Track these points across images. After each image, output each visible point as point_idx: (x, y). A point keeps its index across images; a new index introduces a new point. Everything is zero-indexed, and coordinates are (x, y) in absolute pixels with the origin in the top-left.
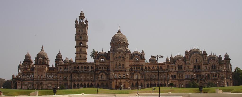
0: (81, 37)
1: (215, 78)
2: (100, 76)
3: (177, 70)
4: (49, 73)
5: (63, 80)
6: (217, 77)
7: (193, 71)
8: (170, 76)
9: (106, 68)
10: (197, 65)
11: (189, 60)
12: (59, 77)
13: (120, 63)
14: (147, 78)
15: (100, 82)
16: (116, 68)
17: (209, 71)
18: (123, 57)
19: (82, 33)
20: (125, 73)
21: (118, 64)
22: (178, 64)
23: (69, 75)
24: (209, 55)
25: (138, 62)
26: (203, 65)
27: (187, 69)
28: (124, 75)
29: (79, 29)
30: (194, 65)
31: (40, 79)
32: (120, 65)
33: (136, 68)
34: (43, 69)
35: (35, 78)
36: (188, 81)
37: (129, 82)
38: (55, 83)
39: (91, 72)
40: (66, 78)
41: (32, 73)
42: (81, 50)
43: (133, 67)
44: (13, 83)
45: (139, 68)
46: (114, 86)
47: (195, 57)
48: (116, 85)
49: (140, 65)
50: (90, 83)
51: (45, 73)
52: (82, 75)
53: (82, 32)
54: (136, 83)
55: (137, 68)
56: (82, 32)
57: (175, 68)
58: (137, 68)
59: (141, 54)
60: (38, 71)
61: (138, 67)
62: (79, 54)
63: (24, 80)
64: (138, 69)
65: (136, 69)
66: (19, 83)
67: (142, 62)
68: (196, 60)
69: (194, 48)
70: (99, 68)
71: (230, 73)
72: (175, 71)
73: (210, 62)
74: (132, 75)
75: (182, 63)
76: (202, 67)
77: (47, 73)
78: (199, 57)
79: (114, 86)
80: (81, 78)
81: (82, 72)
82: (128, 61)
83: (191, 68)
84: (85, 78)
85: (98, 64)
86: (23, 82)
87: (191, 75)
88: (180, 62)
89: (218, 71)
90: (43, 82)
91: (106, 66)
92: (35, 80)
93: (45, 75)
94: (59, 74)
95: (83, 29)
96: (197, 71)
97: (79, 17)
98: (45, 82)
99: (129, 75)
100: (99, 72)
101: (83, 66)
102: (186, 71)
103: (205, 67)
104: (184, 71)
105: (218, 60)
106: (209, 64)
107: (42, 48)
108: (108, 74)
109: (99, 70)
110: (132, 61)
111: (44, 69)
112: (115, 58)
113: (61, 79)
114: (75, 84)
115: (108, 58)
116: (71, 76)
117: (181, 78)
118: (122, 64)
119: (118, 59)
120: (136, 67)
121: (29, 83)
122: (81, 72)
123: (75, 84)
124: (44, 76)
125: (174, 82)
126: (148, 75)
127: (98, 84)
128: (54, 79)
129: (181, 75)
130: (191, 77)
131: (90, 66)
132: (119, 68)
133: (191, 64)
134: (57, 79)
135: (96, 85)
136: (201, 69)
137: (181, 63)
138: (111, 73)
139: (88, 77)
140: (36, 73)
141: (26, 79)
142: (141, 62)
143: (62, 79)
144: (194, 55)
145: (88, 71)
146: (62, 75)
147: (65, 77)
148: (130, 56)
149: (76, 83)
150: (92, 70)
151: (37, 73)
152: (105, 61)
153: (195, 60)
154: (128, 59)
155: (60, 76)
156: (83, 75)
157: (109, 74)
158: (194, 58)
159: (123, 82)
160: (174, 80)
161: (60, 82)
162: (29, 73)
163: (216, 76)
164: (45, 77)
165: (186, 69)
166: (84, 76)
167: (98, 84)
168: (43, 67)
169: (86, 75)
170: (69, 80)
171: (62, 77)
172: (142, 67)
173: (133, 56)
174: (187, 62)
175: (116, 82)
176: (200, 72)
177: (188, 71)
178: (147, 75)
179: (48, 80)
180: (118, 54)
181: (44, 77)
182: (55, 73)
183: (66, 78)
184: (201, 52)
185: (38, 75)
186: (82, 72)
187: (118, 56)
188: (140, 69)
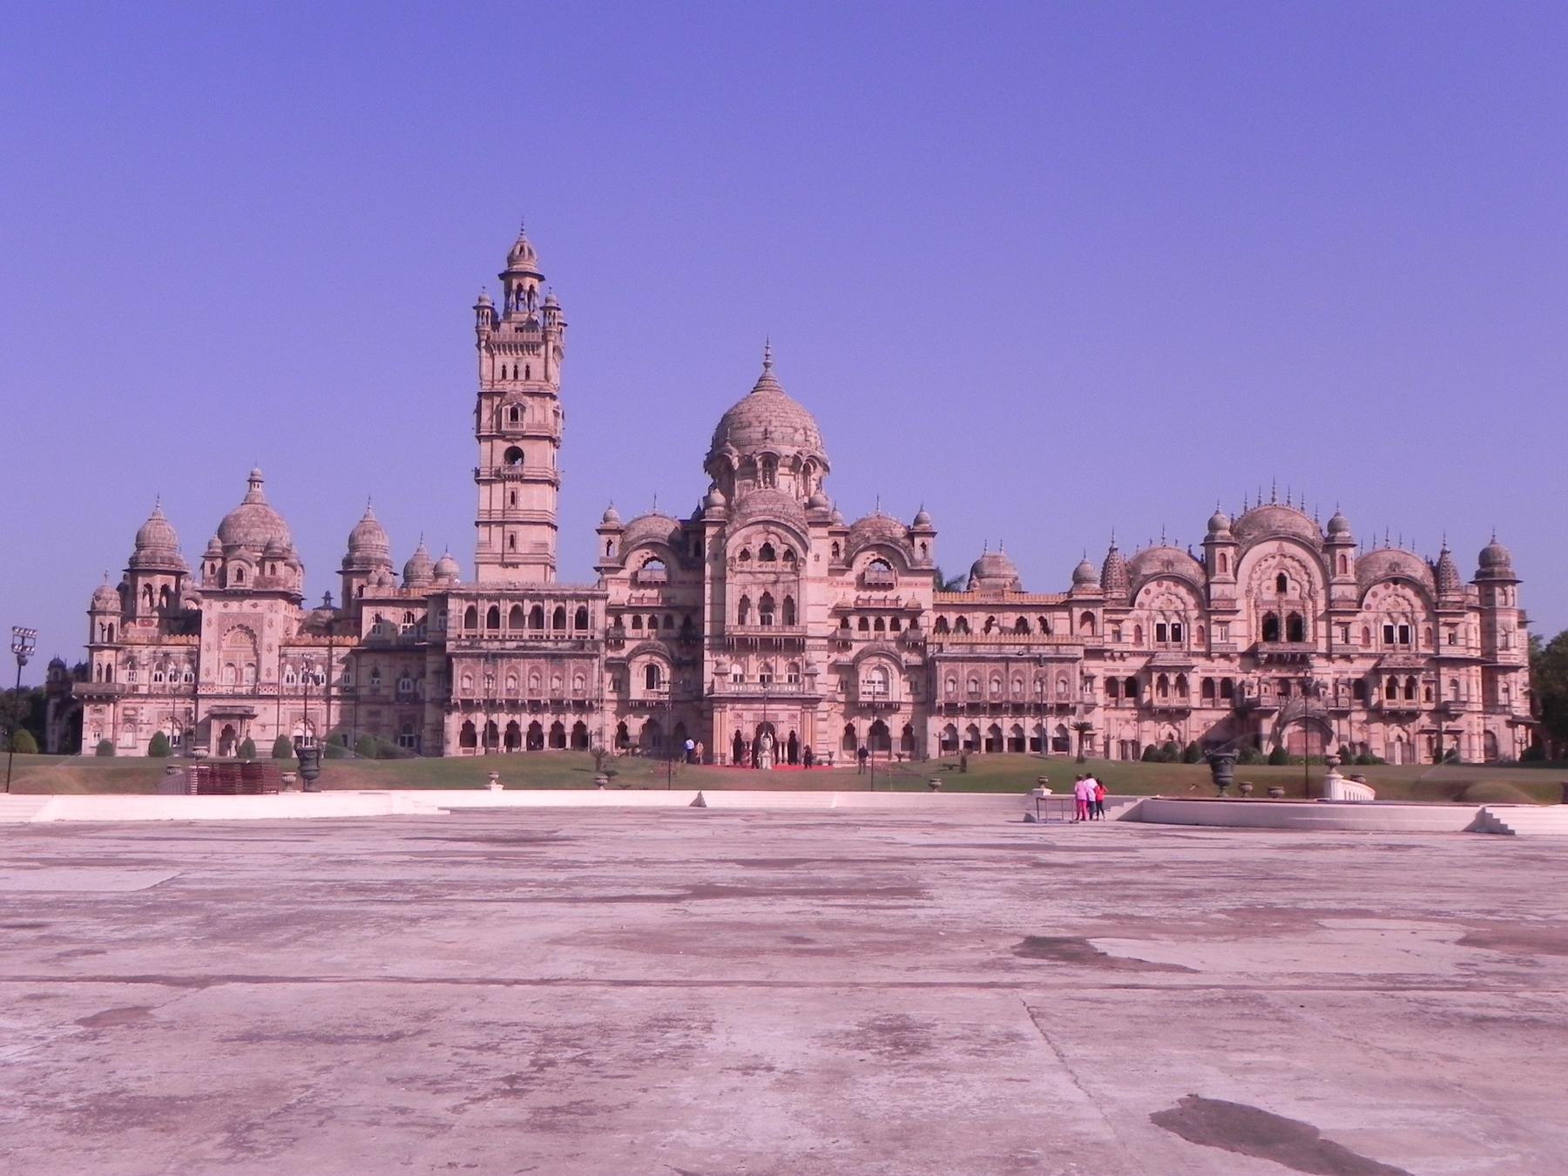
0: (514, 415)
1: (1400, 702)
3: (1150, 642)
4: (297, 650)
5: (392, 698)
6: (1420, 701)
7: (1251, 655)
8: (1099, 683)
9: (678, 621)
10: (1284, 615)
11: (1232, 578)
13: (767, 594)
16: (742, 621)
17: (1362, 655)
18: (789, 554)
19: (520, 388)
21: (755, 599)
22: (1157, 604)
23: (432, 662)
24: (1367, 550)
25: (891, 586)
28: (795, 666)
30: (1262, 613)
32: (767, 604)
33: (872, 627)
34: (260, 617)
35: (203, 678)
37: (825, 715)
39: (581, 643)
40: (415, 681)
41: (184, 649)
42: (513, 501)
43: (854, 621)
44: (58, 714)
45: (895, 625)
46: (723, 746)
47: (1272, 562)
48: (738, 733)
49: (902, 604)
50: (569, 721)
51: (270, 650)
53: (522, 376)
54: (869, 723)
55: (879, 625)
56: (522, 376)
57: (1139, 629)
58: (879, 625)
59: (911, 535)
61: (887, 620)
62: (497, 531)
63: (133, 692)
65: (872, 633)
66: (96, 716)
67: (917, 590)
69: (1266, 500)
70: (627, 619)
71: (1513, 676)
72: (1133, 654)
73: (1375, 595)
74: (848, 674)
76: (1315, 628)
77: (290, 650)
79: (723, 746)
81: (514, 644)
82: (821, 580)
83: (1243, 631)
85: (620, 593)
88: (1173, 589)
89: (1424, 656)
90: (257, 706)
91: (675, 608)
92: (203, 697)
93: (270, 661)
94: (365, 660)
96: (1280, 656)
97: (502, 276)
98: (272, 707)
99: (822, 669)
100: (630, 646)
101: (527, 607)
102: (1208, 656)
103: (1337, 631)
104: (1194, 649)
105: (1430, 582)
106: (1369, 607)
108: (687, 664)
109: (629, 632)
110: (851, 576)
111: (266, 621)
112: (733, 559)
114: (468, 728)
115: (692, 554)
116: (446, 674)
117: (1174, 700)
118: (779, 600)
119: (755, 564)
120: (872, 620)
121: (160, 714)
122: (509, 645)
123: (468, 728)
125: (1127, 722)
126: (954, 672)
127: (622, 728)
129: (1172, 679)
130: (1242, 693)
131: (572, 608)
132: (763, 622)
135: (611, 731)
136: (1310, 639)
137: (1173, 598)
138: (707, 654)
141: (143, 690)
142: (909, 584)
143: (384, 692)
144: (1270, 547)
145: (556, 641)
146: (383, 662)
147: (406, 675)
148: (836, 544)
150: (589, 632)
152: (669, 576)
153: (1273, 583)
154: (822, 568)
155: (370, 668)
156: (525, 666)
157: (698, 664)
159: (783, 716)
160: (1123, 709)
161: (374, 708)
162: (165, 648)
163: (1409, 695)
164: (274, 679)
166: (532, 670)
167: (622, 728)
168: (259, 609)
170: (432, 701)
171: (386, 678)
173: (857, 545)
174: (1216, 590)
175: (740, 716)
176: (1302, 661)
177: (1225, 656)
179: (291, 697)
180: (753, 528)
181: (263, 678)
182: (341, 650)
183: (415, 681)
184: (1309, 533)
185: (222, 664)
186: (514, 644)
187: (755, 550)
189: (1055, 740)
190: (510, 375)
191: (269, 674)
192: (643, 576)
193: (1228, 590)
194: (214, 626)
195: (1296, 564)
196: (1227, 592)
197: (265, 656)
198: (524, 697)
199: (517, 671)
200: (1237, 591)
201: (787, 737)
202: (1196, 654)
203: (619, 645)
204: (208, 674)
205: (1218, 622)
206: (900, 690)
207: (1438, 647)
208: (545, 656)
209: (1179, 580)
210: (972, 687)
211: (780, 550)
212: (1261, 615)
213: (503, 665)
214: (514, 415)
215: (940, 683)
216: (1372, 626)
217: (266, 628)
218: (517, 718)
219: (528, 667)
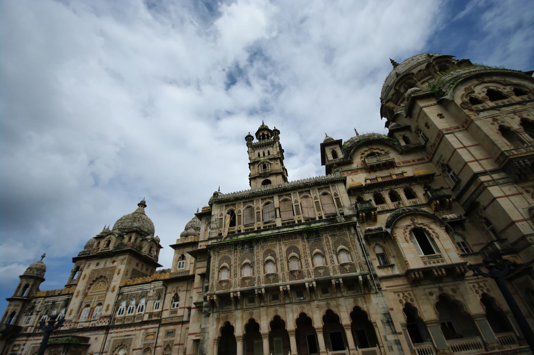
0: (265, 167)
2: (401, 234)
4: (130, 288)
12: (168, 304)
15: (420, 291)
29: (256, 152)
31: (86, 325)
38: (148, 335)
52: (277, 250)
53: (266, 154)
56: (266, 154)
60: (92, 287)
77: (126, 290)
80: (270, 269)
84: (295, 266)
86: (15, 346)
93: (111, 298)
95: (270, 149)
98: (101, 335)
107: (143, 204)
111: (117, 271)
113: (176, 312)
115: (403, 144)
124: (105, 307)
127: (410, 311)
128: (146, 318)
134: (160, 314)
139: (319, 262)
140: (80, 294)
143: (180, 312)
146: (183, 287)
149: (238, 314)
151: (86, 295)
155: (173, 295)
156: (281, 249)
164: (109, 313)
166: (288, 251)
168: (115, 264)
169: (301, 244)
179: (118, 327)
190: (261, 155)
191: (107, 310)
192: (372, 161)
194: (86, 279)
197: (109, 294)
198: (285, 282)
199: (274, 255)
203: (370, 216)
204: (70, 314)
208: (300, 233)
211: (508, 90)
213: (259, 252)
214: (265, 167)
217: (116, 275)
218: (281, 312)
219: (284, 249)
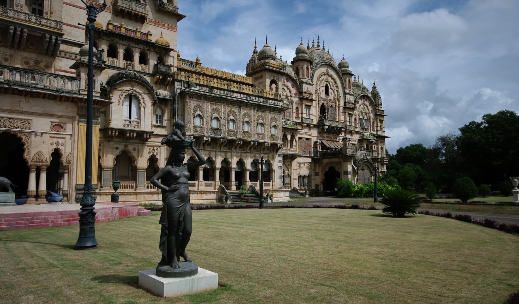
7: (320, 126)
14: (195, 127)
17: (357, 133)
20: (44, 60)
26: (341, 109)
27: (305, 116)
36: (304, 164)
47: (324, 77)
64: (137, 66)
65: (121, 62)
68: (327, 88)
75: (289, 89)
76: (339, 115)
78: (331, 76)
87: (314, 139)
96: (333, 127)
103: (348, 119)
104: (295, 120)
133: (314, 97)
142: (157, 24)
144: (323, 70)
158: (321, 79)
165: (300, 116)
172: (161, 61)
174: (305, 87)
177: (309, 126)
178: (195, 110)
188: (150, 69)
189: (250, 173)
193: (310, 87)
195: (332, 81)
196: (309, 89)
200: (311, 89)
201: (47, 157)
202: (296, 123)
205: (306, 105)
206: (147, 120)
207: (377, 130)
209: (289, 78)
210: (215, 124)
212: (320, 105)
215: (189, 117)
216: (358, 118)
